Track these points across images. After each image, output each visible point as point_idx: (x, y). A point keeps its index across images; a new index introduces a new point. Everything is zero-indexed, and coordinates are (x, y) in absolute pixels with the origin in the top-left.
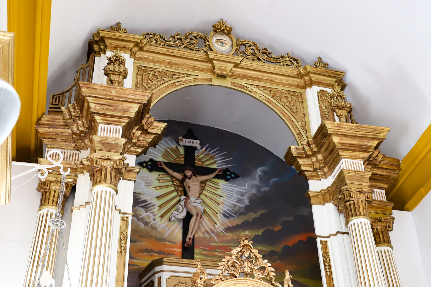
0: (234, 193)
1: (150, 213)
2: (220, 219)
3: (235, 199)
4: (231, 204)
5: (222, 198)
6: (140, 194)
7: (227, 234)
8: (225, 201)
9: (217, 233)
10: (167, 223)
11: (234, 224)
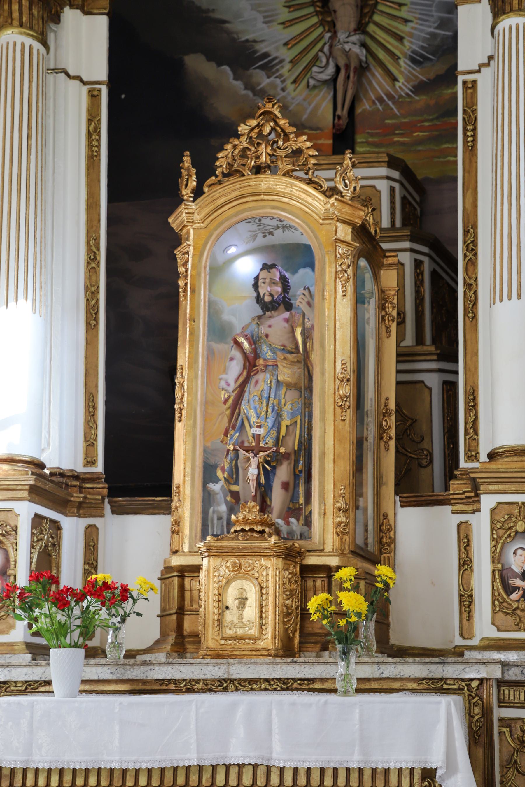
0: (433, 9)
1: (276, 77)
2: (405, 68)
3: (434, 23)
4: (427, 34)
5: (410, 24)
6: (255, 41)
7: (417, 98)
8: (415, 29)
9: (399, 98)
10: (306, 92)
11: (432, 76)
